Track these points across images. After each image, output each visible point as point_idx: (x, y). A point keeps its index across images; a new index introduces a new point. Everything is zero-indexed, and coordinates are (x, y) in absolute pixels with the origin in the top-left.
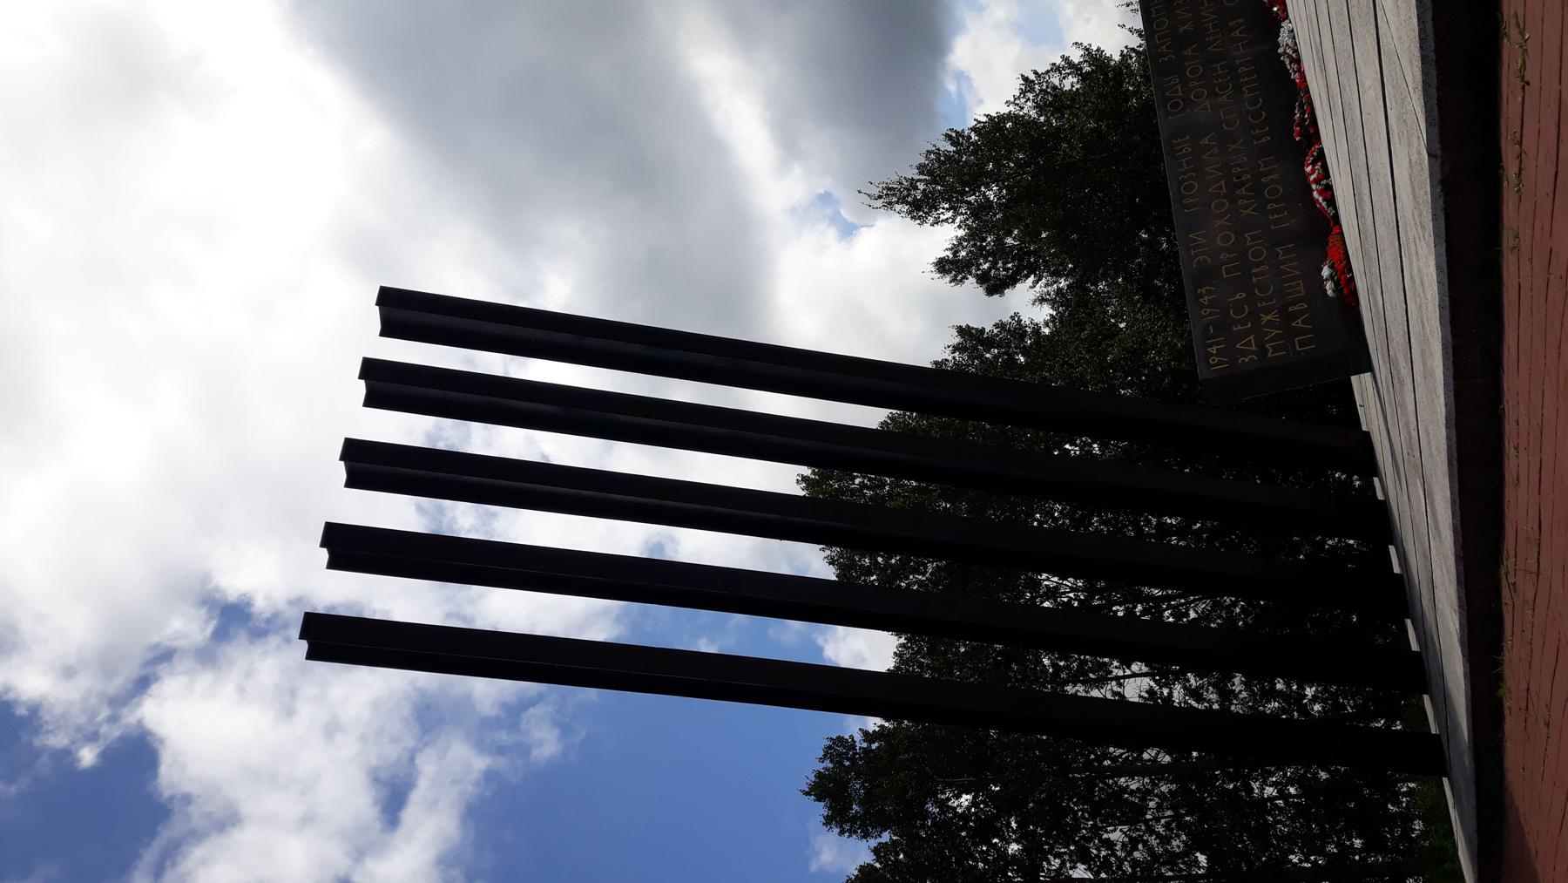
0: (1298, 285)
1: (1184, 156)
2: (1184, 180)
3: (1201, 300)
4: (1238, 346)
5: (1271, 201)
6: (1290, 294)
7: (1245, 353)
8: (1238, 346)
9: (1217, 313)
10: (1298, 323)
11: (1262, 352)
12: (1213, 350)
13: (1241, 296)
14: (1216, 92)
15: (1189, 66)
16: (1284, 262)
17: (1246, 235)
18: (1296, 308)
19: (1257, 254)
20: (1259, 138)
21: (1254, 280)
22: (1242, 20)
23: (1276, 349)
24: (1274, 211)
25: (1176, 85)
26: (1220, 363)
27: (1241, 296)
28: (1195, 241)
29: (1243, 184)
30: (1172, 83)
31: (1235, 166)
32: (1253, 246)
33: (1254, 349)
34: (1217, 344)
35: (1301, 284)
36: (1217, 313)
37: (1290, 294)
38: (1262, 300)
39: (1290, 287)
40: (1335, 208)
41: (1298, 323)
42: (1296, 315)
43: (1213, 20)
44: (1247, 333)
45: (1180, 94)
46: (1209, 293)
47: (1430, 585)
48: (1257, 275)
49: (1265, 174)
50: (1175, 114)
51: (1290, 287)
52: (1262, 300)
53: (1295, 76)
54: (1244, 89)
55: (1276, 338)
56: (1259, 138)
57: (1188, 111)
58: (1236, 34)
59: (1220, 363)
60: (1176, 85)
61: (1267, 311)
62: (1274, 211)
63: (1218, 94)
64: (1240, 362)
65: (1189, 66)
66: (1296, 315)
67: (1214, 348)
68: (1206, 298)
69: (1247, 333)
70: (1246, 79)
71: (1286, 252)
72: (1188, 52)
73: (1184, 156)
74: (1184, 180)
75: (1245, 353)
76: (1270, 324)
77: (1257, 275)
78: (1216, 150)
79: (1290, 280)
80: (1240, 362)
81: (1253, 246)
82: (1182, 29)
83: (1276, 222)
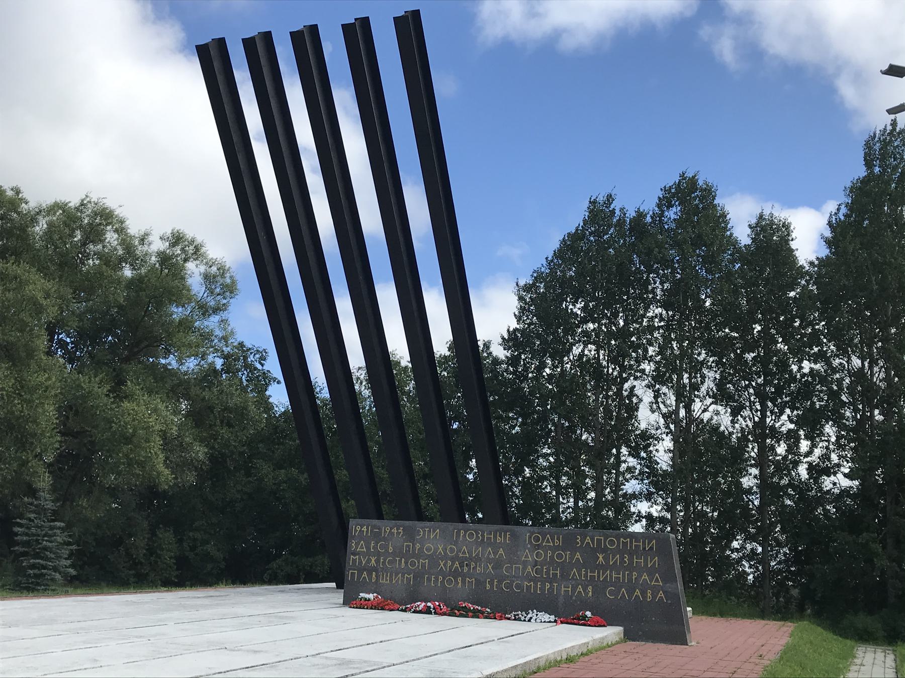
0: (387, 580)
1: (495, 537)
2: (477, 534)
3: (395, 528)
4: (362, 542)
5: (444, 578)
6: (383, 576)
7: (357, 544)
8: (362, 542)
9: (385, 535)
10: (365, 574)
11: (354, 554)
12: (365, 529)
13: (391, 550)
14: (537, 566)
15: (566, 555)
16: (403, 576)
17: (427, 561)
18: (374, 576)
19: (413, 564)
20: (491, 583)
21: (398, 559)
23: (354, 561)
24: (437, 579)
25: (553, 542)
26: (356, 531)
27: (391, 550)
28: (434, 532)
29: (462, 566)
30: (556, 540)
31: (476, 564)
32: (419, 563)
33: (358, 550)
34: (367, 532)
35: (386, 582)
36: (385, 535)
37: (383, 576)
38: (385, 560)
39: (387, 576)
40: (402, 610)
41: (365, 574)
42: (370, 575)
43: (599, 577)
44: (368, 548)
45: (544, 544)
46: (398, 533)
47: (219, 598)
49: (463, 582)
50: (530, 537)
51: (387, 576)
52: (385, 560)
53: (512, 616)
54: (532, 583)
55: (360, 562)
56: (491, 583)
57: (529, 546)
59: (356, 531)
60: (553, 542)
61: (377, 561)
62: (437, 579)
63: (534, 567)
64: (353, 541)
65: (566, 555)
66: (370, 575)
67: (365, 530)
68: (396, 531)
69: (368, 548)
70: (539, 586)
71: (409, 580)
72: (578, 556)
73: (495, 537)
74: (477, 534)
75: (357, 544)
76: (369, 561)
80: (353, 541)
81: (419, 563)
83: (429, 580)
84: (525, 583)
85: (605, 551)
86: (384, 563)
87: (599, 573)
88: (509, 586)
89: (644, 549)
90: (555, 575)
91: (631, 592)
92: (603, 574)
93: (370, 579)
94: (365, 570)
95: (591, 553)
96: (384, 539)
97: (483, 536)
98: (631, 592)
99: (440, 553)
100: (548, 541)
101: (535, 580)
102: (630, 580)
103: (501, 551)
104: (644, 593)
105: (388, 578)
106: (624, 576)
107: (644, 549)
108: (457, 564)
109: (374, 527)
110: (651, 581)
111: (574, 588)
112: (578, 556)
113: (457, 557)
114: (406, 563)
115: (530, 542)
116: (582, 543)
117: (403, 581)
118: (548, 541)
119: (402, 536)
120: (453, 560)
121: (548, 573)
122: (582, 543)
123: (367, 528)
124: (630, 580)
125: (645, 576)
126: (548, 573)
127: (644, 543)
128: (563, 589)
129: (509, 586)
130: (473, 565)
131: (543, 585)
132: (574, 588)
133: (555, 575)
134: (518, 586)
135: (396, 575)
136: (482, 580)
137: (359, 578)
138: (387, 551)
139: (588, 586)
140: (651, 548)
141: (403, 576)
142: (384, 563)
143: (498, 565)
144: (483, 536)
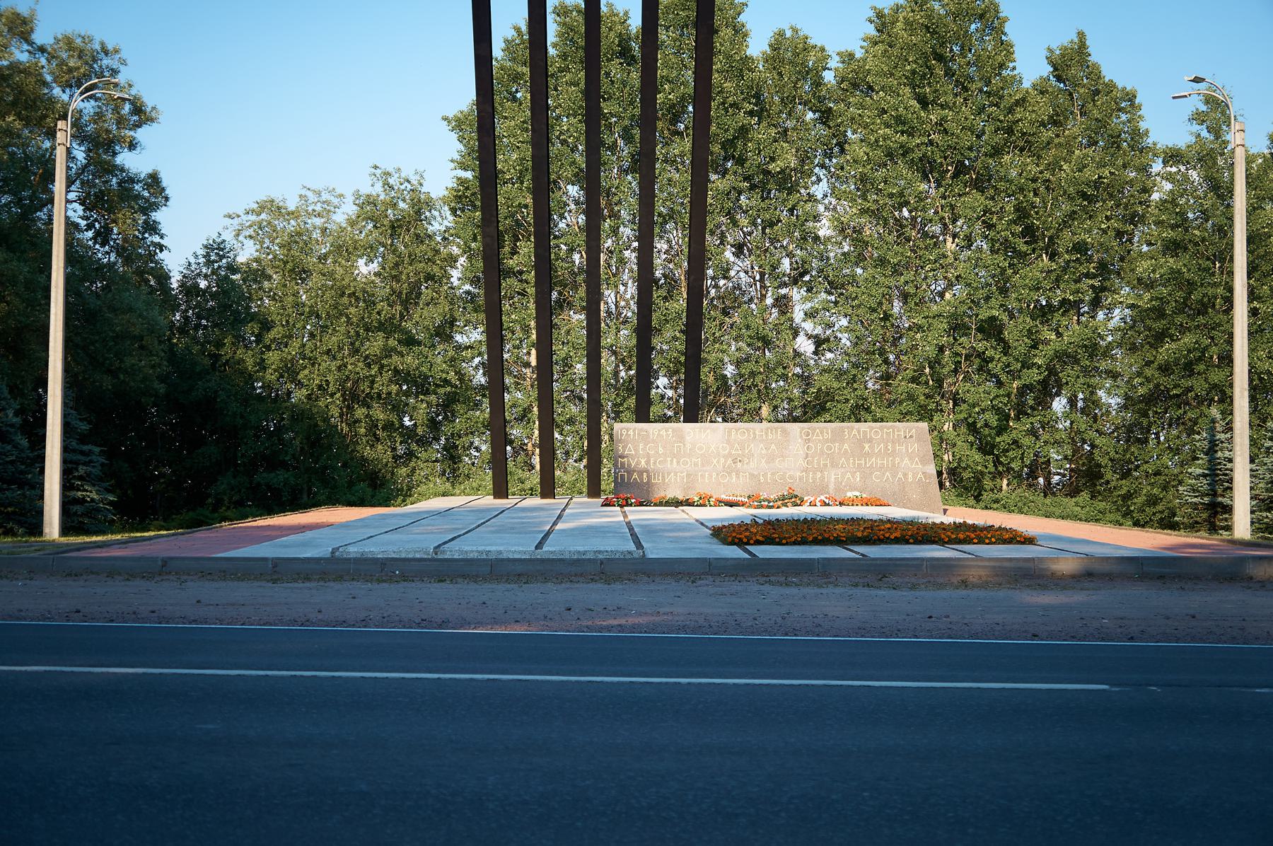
1: (766, 434)
11: (623, 457)
13: (661, 450)
16: (676, 475)
18: (645, 476)
21: (669, 459)
22: (858, 479)
23: (623, 464)
26: (622, 435)
27: (661, 450)
34: (634, 435)
37: (655, 474)
48: (672, 461)
49: (738, 478)
51: (659, 476)
55: (629, 465)
56: (765, 475)
57: (800, 440)
58: (849, 475)
60: (823, 436)
61: (648, 462)
73: (766, 434)
77: (672, 461)
78: (764, 452)
79: (663, 477)
82: (867, 446)
84: (798, 474)
85: (870, 441)
86: (655, 463)
87: (865, 460)
88: (783, 477)
89: (905, 437)
90: (825, 465)
91: (894, 476)
92: (869, 461)
93: (642, 479)
94: (635, 471)
95: (860, 443)
96: (653, 441)
97: (754, 433)
98: (894, 476)
99: (713, 452)
100: (817, 435)
101: (806, 470)
102: (893, 465)
103: (773, 446)
104: (905, 475)
105: (660, 478)
106: (888, 461)
107: (905, 437)
108: (730, 461)
109: (642, 430)
110: (912, 464)
111: (844, 474)
112: (846, 446)
113: (730, 454)
114: (678, 462)
115: (801, 436)
116: (850, 436)
117: (676, 479)
118: (817, 435)
119: (672, 437)
120: (726, 457)
121: (819, 465)
122: (850, 436)
123: (634, 431)
124: (893, 465)
125: (906, 461)
126: (819, 463)
127: (905, 432)
128: (833, 477)
129: (783, 477)
130: (746, 460)
131: (814, 473)
132: (844, 474)
133: (825, 465)
134: (791, 477)
135: (669, 474)
136: (756, 473)
137: (629, 479)
138: (657, 452)
139: (855, 472)
140: (911, 437)
141: (676, 475)
142: (655, 463)
143: (770, 459)
144: (754, 433)
